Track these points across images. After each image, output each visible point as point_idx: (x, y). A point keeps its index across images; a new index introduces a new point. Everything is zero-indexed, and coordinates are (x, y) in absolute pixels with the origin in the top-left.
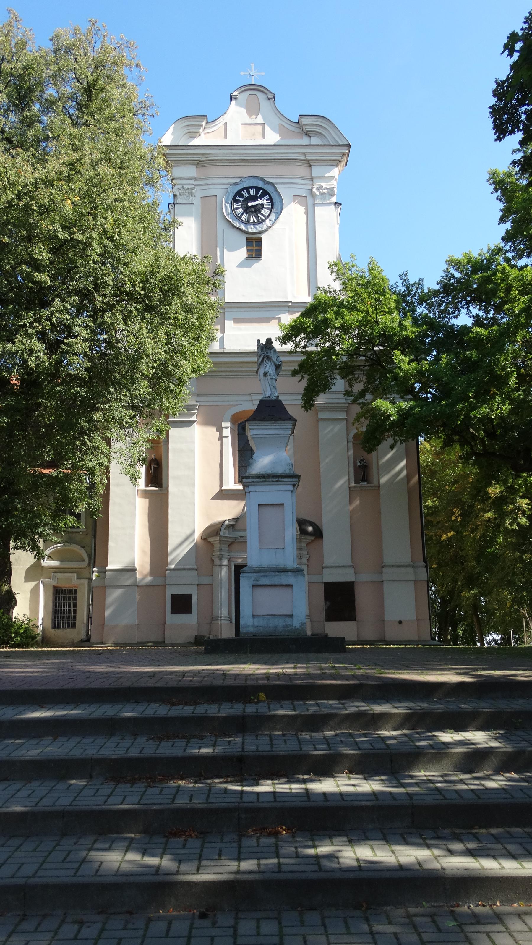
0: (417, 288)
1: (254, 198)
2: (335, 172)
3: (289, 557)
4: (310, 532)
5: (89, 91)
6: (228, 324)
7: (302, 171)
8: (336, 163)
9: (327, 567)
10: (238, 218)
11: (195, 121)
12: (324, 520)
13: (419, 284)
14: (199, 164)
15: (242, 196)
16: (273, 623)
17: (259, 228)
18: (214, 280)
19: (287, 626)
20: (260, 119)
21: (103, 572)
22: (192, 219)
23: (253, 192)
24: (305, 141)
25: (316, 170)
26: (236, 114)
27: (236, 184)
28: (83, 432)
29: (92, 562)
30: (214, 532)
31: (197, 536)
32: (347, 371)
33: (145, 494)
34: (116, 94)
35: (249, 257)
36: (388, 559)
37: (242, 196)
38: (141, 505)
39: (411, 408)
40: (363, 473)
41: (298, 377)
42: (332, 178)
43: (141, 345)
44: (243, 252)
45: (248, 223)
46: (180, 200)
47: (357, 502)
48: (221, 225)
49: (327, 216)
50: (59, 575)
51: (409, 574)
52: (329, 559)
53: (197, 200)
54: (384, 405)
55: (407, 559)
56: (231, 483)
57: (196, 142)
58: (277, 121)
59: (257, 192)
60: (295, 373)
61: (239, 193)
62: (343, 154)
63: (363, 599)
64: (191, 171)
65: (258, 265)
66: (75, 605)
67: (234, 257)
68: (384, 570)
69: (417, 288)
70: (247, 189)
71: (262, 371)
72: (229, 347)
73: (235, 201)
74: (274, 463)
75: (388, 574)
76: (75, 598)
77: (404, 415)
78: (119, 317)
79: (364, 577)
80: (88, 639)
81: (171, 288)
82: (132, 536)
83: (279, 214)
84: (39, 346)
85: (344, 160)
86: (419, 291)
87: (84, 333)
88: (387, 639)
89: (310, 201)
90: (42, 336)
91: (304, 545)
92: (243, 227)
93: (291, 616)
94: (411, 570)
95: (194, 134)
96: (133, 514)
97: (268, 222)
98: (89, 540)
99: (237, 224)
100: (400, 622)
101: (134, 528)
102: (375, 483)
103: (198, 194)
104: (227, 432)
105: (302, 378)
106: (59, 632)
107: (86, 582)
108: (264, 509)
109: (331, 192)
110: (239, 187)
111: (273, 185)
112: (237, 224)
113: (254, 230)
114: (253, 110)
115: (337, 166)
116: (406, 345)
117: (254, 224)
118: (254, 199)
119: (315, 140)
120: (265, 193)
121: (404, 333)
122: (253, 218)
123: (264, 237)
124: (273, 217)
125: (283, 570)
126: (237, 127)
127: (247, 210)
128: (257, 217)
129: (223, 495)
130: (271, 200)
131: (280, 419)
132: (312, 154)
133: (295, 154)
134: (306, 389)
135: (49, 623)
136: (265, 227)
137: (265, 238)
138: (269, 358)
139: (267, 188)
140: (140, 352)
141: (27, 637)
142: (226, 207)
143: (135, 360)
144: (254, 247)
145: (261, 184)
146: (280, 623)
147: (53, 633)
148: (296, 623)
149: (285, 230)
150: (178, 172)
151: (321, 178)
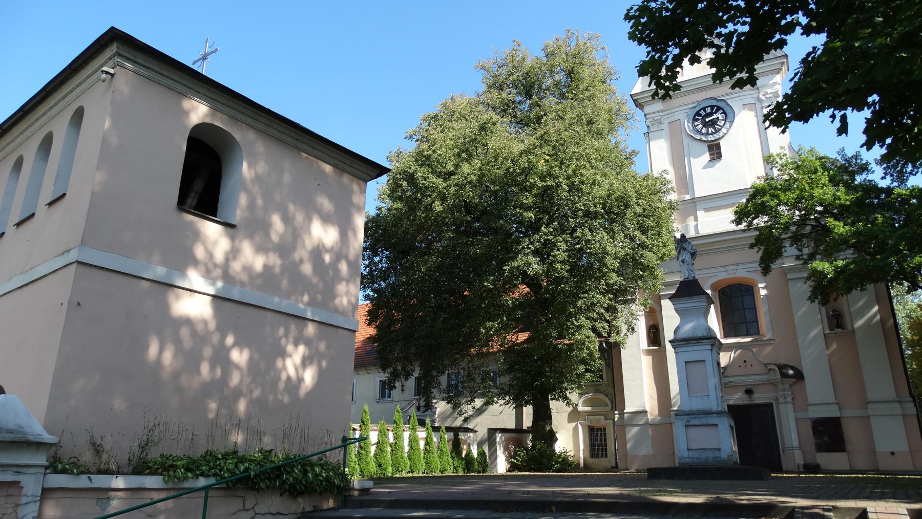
0: (856, 159)
1: (711, 114)
6: (700, 213)
8: (778, 71)
9: (811, 405)
10: (700, 132)
12: (803, 364)
13: (857, 156)
15: (700, 115)
16: (704, 455)
17: (716, 136)
18: (685, 182)
19: (716, 458)
21: (622, 414)
22: (663, 140)
23: (709, 110)
27: (694, 107)
28: (571, 315)
29: (614, 408)
32: (796, 239)
33: (648, 352)
35: (712, 160)
37: (700, 115)
38: (646, 363)
39: (847, 265)
40: (837, 321)
41: (756, 249)
42: (776, 83)
43: (604, 249)
44: (707, 157)
45: (707, 134)
46: (652, 129)
47: (834, 346)
48: (686, 140)
50: (591, 417)
51: (897, 408)
53: (665, 126)
55: (892, 395)
59: (712, 110)
60: (752, 246)
61: (698, 114)
62: (783, 63)
63: (851, 432)
65: (719, 165)
66: (605, 440)
67: (699, 162)
68: (869, 406)
69: (856, 159)
70: (704, 109)
71: (680, 259)
72: (703, 231)
73: (695, 120)
74: (694, 328)
75: (872, 409)
76: (605, 434)
77: (839, 272)
78: (587, 231)
79: (848, 413)
80: (617, 467)
82: (642, 385)
83: (732, 122)
84: (533, 260)
85: (784, 68)
86: (859, 161)
87: (564, 247)
88: (881, 468)
90: (536, 253)
91: (787, 386)
92: (704, 138)
93: (719, 450)
94: (897, 405)
96: (641, 368)
97: (724, 130)
98: (610, 390)
99: (698, 137)
100: (893, 453)
101: (642, 379)
102: (849, 327)
103: (666, 122)
105: (760, 249)
106: (595, 460)
107: (611, 422)
108: (691, 366)
110: (697, 109)
111: (724, 101)
112: (698, 137)
113: (713, 139)
115: (778, 73)
116: (842, 213)
117: (712, 133)
120: (719, 108)
121: (838, 202)
122: (711, 130)
123: (722, 142)
124: (727, 125)
125: (709, 413)
127: (705, 125)
128: (714, 128)
130: (724, 112)
131: (696, 295)
134: (762, 258)
135: (588, 454)
136: (721, 134)
137: (722, 143)
138: (685, 249)
139: (719, 104)
141: (565, 464)
142: (688, 126)
144: (715, 151)
145: (714, 103)
146: (710, 455)
147: (592, 461)
148: (724, 455)
150: (647, 109)
151: (765, 86)
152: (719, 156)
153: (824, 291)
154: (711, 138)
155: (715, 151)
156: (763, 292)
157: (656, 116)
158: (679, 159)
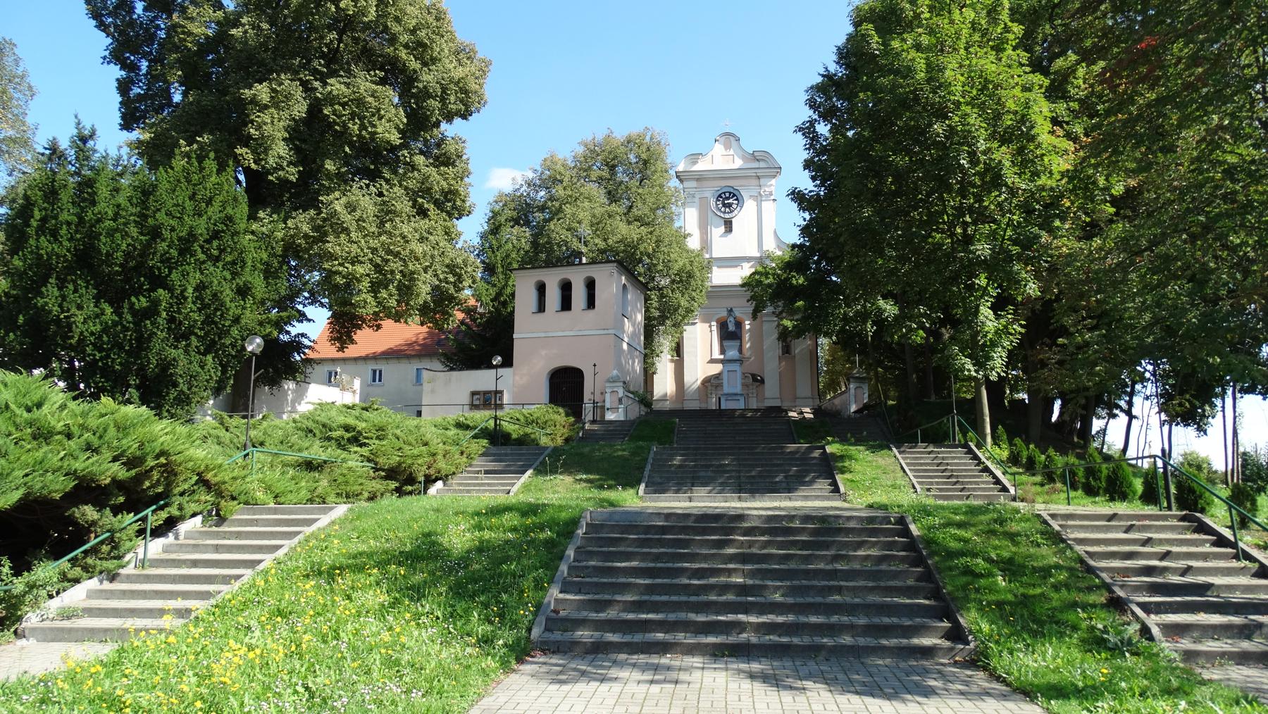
1: (728, 198)
2: (773, 181)
3: (738, 389)
5: (646, 162)
6: (715, 269)
7: (755, 182)
8: (774, 177)
11: (694, 158)
14: (698, 180)
18: (706, 244)
20: (732, 152)
24: (756, 165)
25: (762, 181)
26: (719, 149)
30: (707, 381)
31: (699, 382)
33: (672, 361)
34: (659, 165)
36: (800, 393)
40: (787, 350)
44: (722, 229)
48: (710, 214)
49: (767, 206)
52: (767, 394)
53: (697, 200)
54: (787, 323)
56: (717, 355)
57: (695, 168)
58: (741, 153)
61: (720, 196)
64: (694, 184)
65: (730, 236)
81: (690, 275)
89: (759, 198)
95: (695, 163)
103: (697, 196)
104: (714, 328)
109: (771, 194)
114: (727, 147)
118: (729, 199)
119: (762, 165)
126: (720, 159)
127: (724, 205)
129: (712, 361)
132: (760, 172)
133: (751, 173)
140: (679, 306)
142: (712, 202)
143: (676, 310)
149: (745, 216)
150: (687, 184)
152: (731, 231)
153: (784, 335)
154: (727, 216)
155: (728, 225)
156: (748, 327)
158: (704, 226)
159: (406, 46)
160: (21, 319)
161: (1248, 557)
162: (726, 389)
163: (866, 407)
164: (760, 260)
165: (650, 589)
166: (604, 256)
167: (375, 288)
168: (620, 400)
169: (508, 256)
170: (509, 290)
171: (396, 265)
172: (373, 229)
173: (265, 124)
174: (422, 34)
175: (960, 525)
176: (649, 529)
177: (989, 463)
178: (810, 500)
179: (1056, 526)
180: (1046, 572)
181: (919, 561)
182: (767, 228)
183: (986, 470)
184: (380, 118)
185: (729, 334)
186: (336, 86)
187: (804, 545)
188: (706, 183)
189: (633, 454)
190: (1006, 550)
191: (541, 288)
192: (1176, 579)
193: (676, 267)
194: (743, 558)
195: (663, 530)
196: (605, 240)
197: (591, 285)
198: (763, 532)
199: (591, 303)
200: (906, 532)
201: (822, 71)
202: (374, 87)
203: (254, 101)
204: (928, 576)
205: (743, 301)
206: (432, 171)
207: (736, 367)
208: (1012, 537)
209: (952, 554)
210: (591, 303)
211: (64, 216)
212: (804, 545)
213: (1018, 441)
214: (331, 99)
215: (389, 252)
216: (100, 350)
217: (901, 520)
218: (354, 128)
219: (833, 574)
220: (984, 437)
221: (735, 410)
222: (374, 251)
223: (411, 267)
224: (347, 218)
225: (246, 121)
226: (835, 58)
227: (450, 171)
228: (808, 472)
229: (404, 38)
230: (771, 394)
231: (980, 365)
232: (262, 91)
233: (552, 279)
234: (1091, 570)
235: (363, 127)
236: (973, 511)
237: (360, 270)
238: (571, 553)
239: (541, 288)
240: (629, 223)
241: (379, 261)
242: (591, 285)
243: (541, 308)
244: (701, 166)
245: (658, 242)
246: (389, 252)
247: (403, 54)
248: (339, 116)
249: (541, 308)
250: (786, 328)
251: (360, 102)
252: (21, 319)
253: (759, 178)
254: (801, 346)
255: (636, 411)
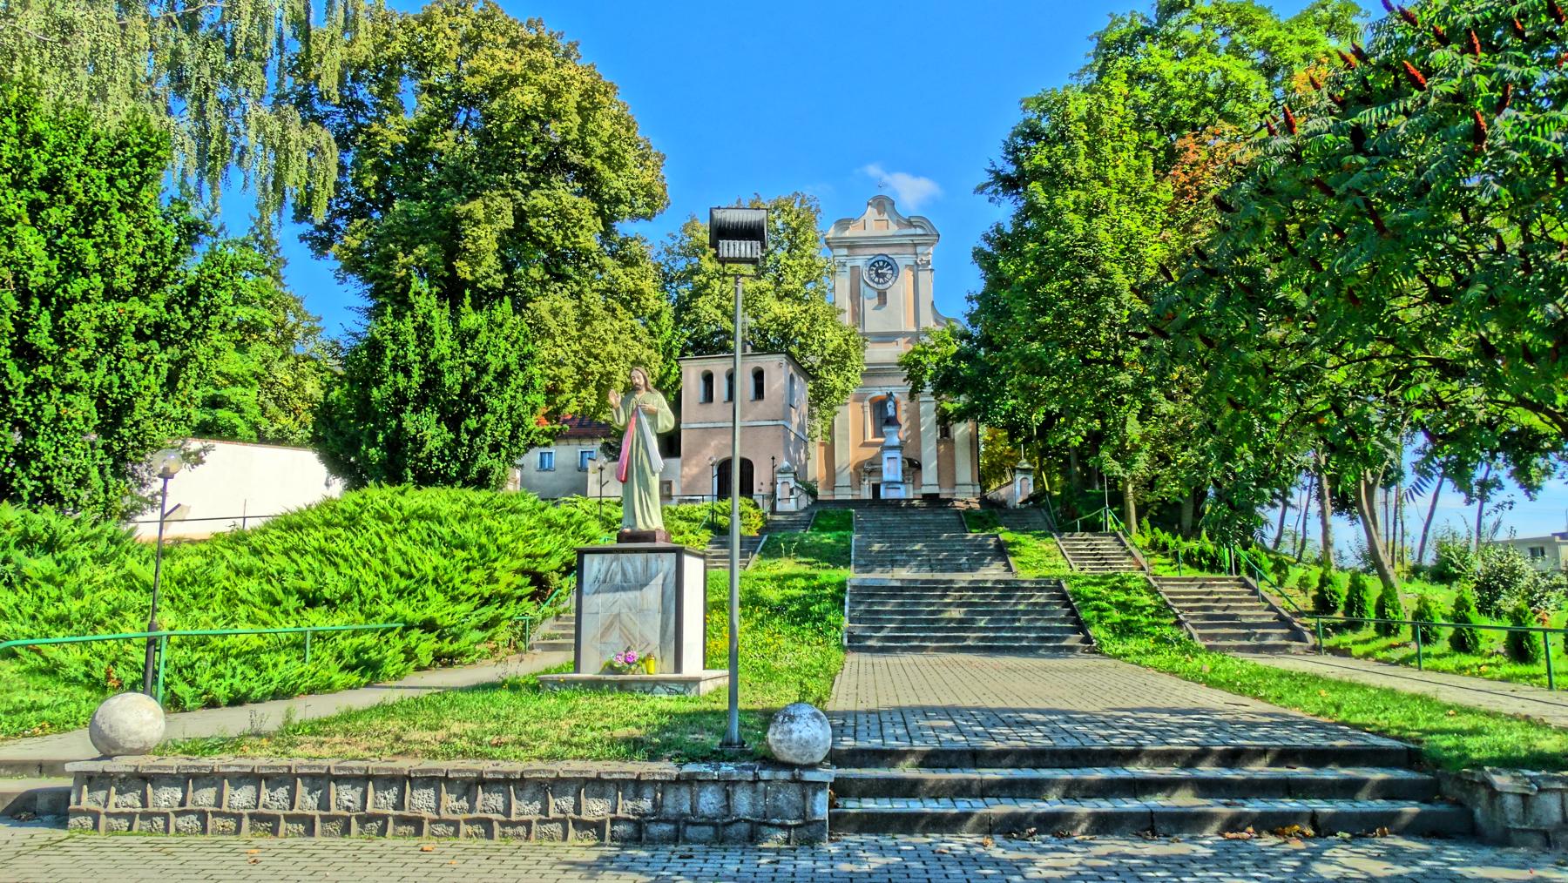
2: (931, 250)
4: (913, 467)
5: (795, 231)
7: (910, 250)
20: (886, 217)
24: (912, 231)
25: (919, 249)
26: (871, 212)
36: (960, 480)
40: (945, 433)
49: (924, 276)
55: (969, 480)
56: (870, 438)
57: (847, 234)
64: (845, 251)
77: (956, 410)
103: (849, 265)
104: (868, 409)
118: (883, 268)
119: (919, 231)
126: (872, 224)
127: (878, 275)
129: (865, 445)
132: (917, 240)
143: (832, 392)
149: (901, 288)
155: (882, 296)
157: (843, 259)
159: (601, 157)
160: (380, 438)
161: (1264, 600)
162: (887, 477)
163: (1031, 498)
164: (915, 337)
165: (903, 621)
166: (762, 345)
167: (577, 388)
168: (791, 492)
169: (669, 343)
170: (672, 379)
171: (595, 367)
172: (575, 333)
173: (480, 238)
174: (615, 145)
175: (1095, 584)
176: (892, 588)
177: (1133, 549)
178: (992, 572)
179: (1155, 584)
180: (1142, 609)
181: (1069, 604)
182: (928, 303)
183: (1130, 553)
184: (582, 228)
185: (883, 417)
186: (539, 199)
187: (996, 597)
188: (858, 251)
189: (838, 541)
190: (1122, 597)
191: (708, 378)
192: (1217, 612)
193: (831, 347)
194: (959, 605)
195: (901, 589)
196: (755, 317)
197: (759, 375)
198: (967, 589)
199: (759, 392)
200: (1060, 589)
201: (989, 166)
202: (576, 198)
203: (469, 216)
204: (1073, 612)
205: (899, 380)
206: (620, 272)
207: (896, 454)
208: (1127, 591)
209: (1088, 600)
210: (759, 392)
211: (411, 356)
212: (996, 597)
213: (1157, 530)
214: (536, 212)
215: (590, 354)
216: (443, 461)
217: (1058, 582)
218: (558, 240)
219: (1015, 612)
220: (1129, 527)
221: (899, 500)
222: (576, 353)
223: (609, 368)
224: (552, 324)
225: (457, 235)
226: (1002, 153)
227: (635, 270)
228: (985, 556)
229: (600, 150)
230: (929, 479)
231: (1126, 467)
232: (477, 207)
233: (719, 367)
234: (1169, 607)
235: (565, 237)
236: (1105, 577)
237: (564, 372)
238: (847, 600)
239: (708, 378)
240: (780, 299)
241: (581, 363)
242: (759, 375)
243: (709, 397)
244: (851, 233)
245: (814, 320)
246: (590, 354)
247: (598, 165)
248: (544, 227)
249: (709, 397)
250: (944, 410)
251: (563, 214)
252: (380, 438)
253: (915, 245)
254: (961, 430)
255: (805, 501)
